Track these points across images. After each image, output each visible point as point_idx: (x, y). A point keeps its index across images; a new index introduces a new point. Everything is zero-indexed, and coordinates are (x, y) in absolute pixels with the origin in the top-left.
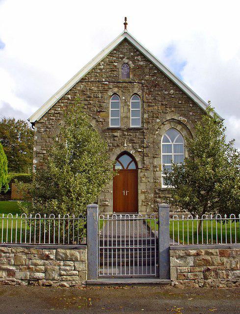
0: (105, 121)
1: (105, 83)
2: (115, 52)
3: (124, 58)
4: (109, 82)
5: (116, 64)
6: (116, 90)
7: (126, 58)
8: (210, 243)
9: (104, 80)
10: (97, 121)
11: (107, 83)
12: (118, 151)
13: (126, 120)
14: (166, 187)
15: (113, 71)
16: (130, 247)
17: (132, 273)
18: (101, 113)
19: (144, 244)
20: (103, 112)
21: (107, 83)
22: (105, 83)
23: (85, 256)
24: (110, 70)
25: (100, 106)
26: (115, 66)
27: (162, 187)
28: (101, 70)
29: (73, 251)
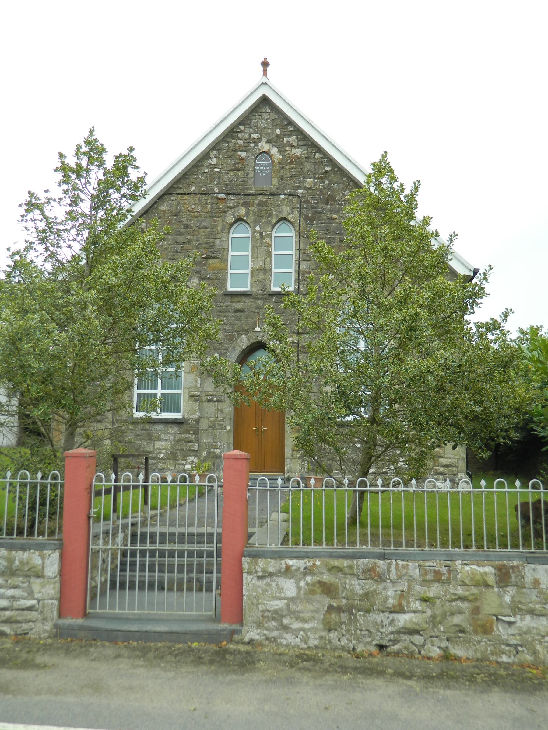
0: (220, 279)
1: (220, 196)
2: (242, 127)
3: (260, 140)
4: (227, 194)
5: (243, 154)
6: (242, 211)
7: (264, 140)
8: (341, 541)
9: (216, 190)
10: (202, 279)
11: (223, 196)
12: (244, 342)
13: (261, 276)
14: (141, 415)
15: (238, 170)
16: (138, 547)
17: (132, 607)
18: (210, 261)
19: (153, 542)
20: (213, 258)
21: (223, 196)
22: (220, 196)
23: (51, 563)
24: (232, 167)
25: (211, 247)
26: (242, 159)
27: (135, 416)
28: (211, 167)
29: (25, 555)
